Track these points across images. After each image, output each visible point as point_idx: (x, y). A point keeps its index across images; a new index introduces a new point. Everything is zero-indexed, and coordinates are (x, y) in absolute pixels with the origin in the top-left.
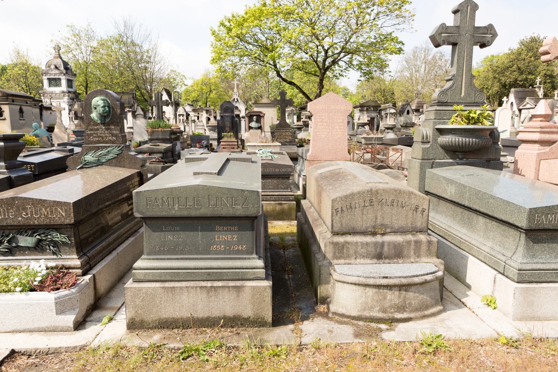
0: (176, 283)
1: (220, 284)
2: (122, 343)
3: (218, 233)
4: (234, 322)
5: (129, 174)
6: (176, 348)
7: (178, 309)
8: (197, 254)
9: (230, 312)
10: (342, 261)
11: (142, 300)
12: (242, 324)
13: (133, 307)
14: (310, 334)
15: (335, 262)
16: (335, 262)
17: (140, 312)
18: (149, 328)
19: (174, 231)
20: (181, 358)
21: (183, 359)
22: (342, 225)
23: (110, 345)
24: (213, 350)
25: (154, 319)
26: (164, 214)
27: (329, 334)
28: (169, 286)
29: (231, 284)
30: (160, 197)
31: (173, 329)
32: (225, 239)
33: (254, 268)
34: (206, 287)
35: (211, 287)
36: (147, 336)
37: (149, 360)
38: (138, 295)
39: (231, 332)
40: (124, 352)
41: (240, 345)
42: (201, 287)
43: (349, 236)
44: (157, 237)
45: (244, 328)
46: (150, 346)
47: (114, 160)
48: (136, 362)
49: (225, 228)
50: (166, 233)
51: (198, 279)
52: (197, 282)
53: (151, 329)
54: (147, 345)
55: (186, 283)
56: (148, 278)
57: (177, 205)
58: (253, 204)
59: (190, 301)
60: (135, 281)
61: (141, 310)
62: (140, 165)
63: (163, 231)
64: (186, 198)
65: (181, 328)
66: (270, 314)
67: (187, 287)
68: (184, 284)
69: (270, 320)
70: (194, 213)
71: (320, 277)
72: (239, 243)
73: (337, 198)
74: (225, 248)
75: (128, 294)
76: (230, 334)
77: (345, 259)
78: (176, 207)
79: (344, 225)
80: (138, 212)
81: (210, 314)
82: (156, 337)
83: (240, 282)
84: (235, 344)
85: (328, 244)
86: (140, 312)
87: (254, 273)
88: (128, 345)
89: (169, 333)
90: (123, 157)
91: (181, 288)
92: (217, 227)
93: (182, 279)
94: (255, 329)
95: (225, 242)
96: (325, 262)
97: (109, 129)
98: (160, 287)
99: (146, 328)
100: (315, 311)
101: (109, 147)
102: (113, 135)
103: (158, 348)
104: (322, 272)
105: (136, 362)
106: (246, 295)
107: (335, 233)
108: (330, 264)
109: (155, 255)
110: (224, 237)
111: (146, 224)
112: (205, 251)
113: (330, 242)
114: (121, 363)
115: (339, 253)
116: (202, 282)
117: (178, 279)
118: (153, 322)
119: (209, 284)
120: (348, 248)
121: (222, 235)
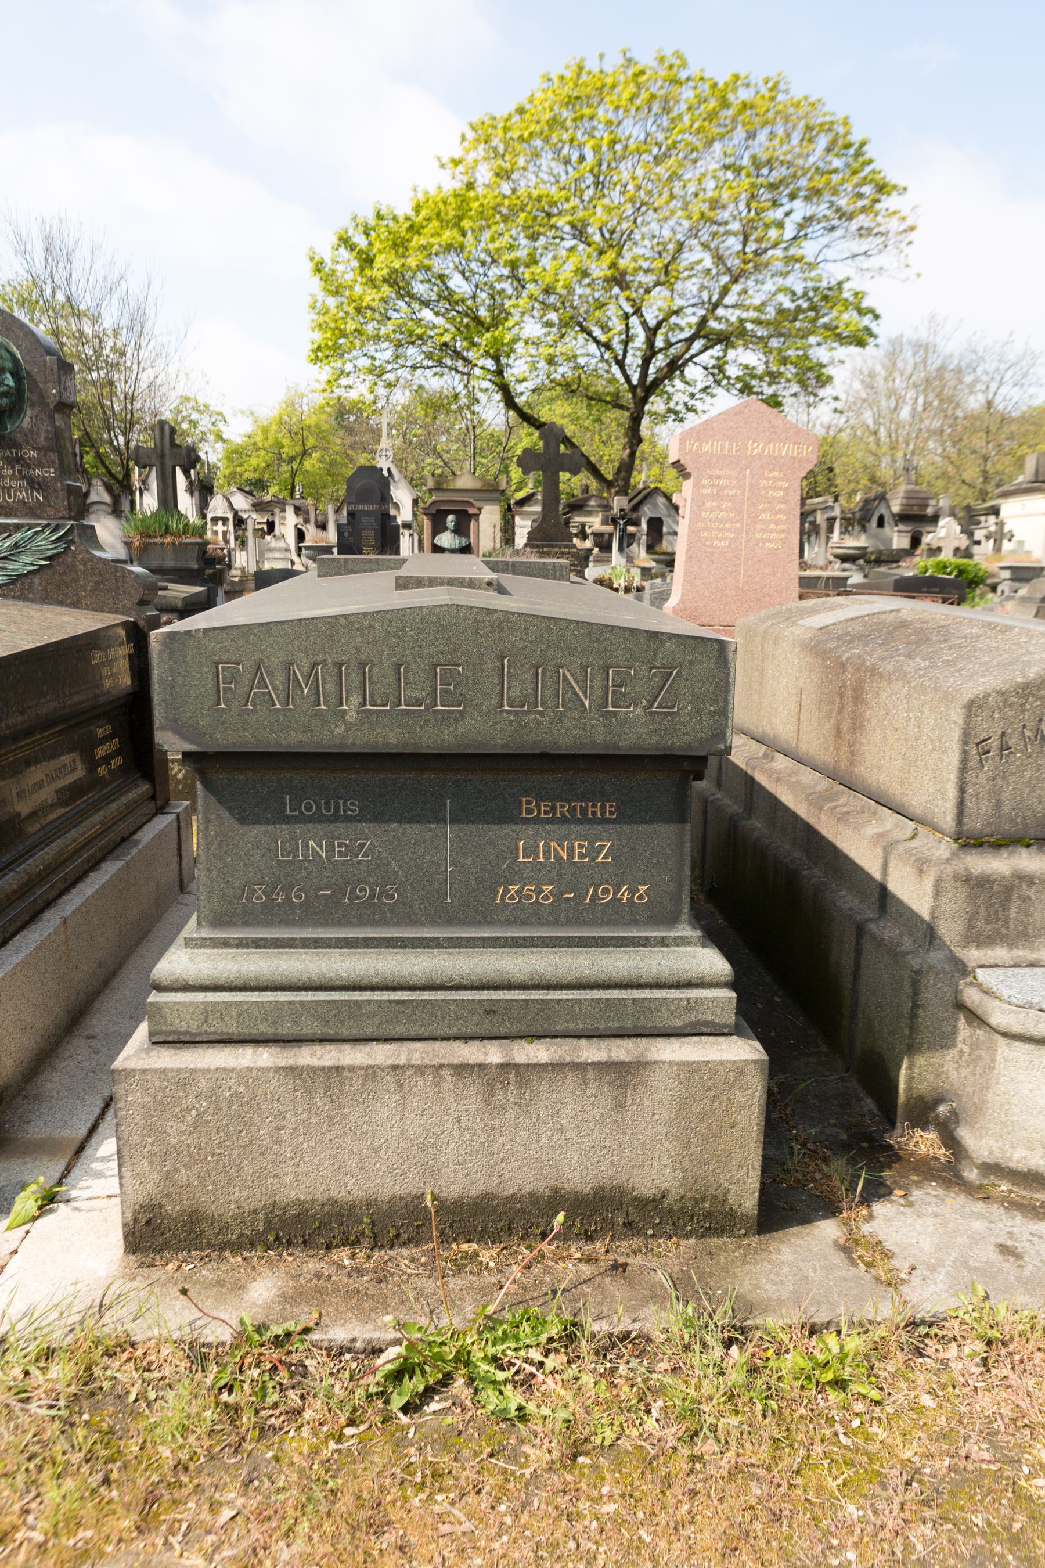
0: (347, 1048)
1: (540, 1052)
2: (113, 1324)
3: (531, 830)
4: (606, 1215)
5: (99, 626)
6: (359, 1345)
7: (352, 1163)
8: (433, 921)
9: (579, 1170)
10: (1000, 953)
11: (195, 1125)
12: (628, 1225)
13: (152, 1155)
14: (932, 1269)
15: (972, 955)
16: (972, 955)
17: (183, 1175)
18: (222, 1247)
19: (335, 819)
20: (398, 1401)
21: (405, 1409)
22: (998, 805)
23: (57, 1337)
24: (535, 1355)
25: (247, 1207)
26: (294, 739)
27: (1008, 1265)
28: (315, 1062)
29: (592, 1052)
30: (276, 662)
31: (329, 1248)
32: (558, 857)
33: (689, 985)
34: (481, 1066)
35: (505, 1067)
36: (220, 1283)
37: (247, 1419)
38: (177, 1101)
39: (589, 1260)
40: (122, 1372)
41: (647, 1327)
42: (461, 1069)
43: (1024, 852)
44: (257, 845)
45: (636, 1242)
46: (241, 1338)
47: (36, 580)
48: (185, 1430)
49: (562, 809)
50: (298, 829)
51: (441, 1032)
52: (438, 1045)
53: (235, 1247)
54: (226, 1335)
55: (387, 1047)
56: (217, 1027)
57: (355, 700)
58: (695, 698)
59: (410, 1128)
60: (160, 1040)
61: (188, 1167)
62: (136, 598)
63: (287, 820)
64: (399, 666)
65: (366, 1243)
66: (753, 1181)
67: (395, 1067)
68: (381, 1054)
69: (750, 1204)
70: (431, 738)
71: (913, 1015)
72: (621, 871)
73: (986, 696)
74: (557, 894)
75: (132, 1101)
76: (586, 1270)
77: (1011, 946)
78: (351, 706)
79: (1006, 809)
80: (177, 728)
81: (492, 1185)
82: (262, 1290)
83: (629, 1044)
84: (625, 1324)
85: (948, 884)
86: (183, 1175)
87: (689, 1006)
88: (139, 1332)
89: (312, 1265)
90: (72, 567)
91: (371, 1072)
92: (529, 805)
93: (370, 1031)
94: (684, 1243)
95: (563, 872)
96: (935, 957)
97: (18, 460)
98: (278, 1070)
99: (210, 1245)
100: (899, 1159)
101: (18, 527)
102: (33, 484)
103: (277, 1349)
104: (927, 996)
105: (185, 1430)
106: (656, 1102)
107: (969, 841)
108: (962, 969)
109: (246, 924)
110: (550, 847)
111: (206, 784)
112: (470, 909)
113: (956, 877)
114: (111, 1431)
115: (988, 922)
116: (458, 1045)
117: (354, 1033)
118: (240, 1217)
119: (493, 1054)
120: (1026, 899)
121: (547, 840)
